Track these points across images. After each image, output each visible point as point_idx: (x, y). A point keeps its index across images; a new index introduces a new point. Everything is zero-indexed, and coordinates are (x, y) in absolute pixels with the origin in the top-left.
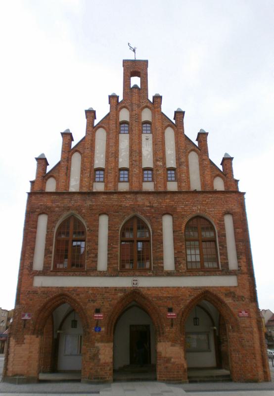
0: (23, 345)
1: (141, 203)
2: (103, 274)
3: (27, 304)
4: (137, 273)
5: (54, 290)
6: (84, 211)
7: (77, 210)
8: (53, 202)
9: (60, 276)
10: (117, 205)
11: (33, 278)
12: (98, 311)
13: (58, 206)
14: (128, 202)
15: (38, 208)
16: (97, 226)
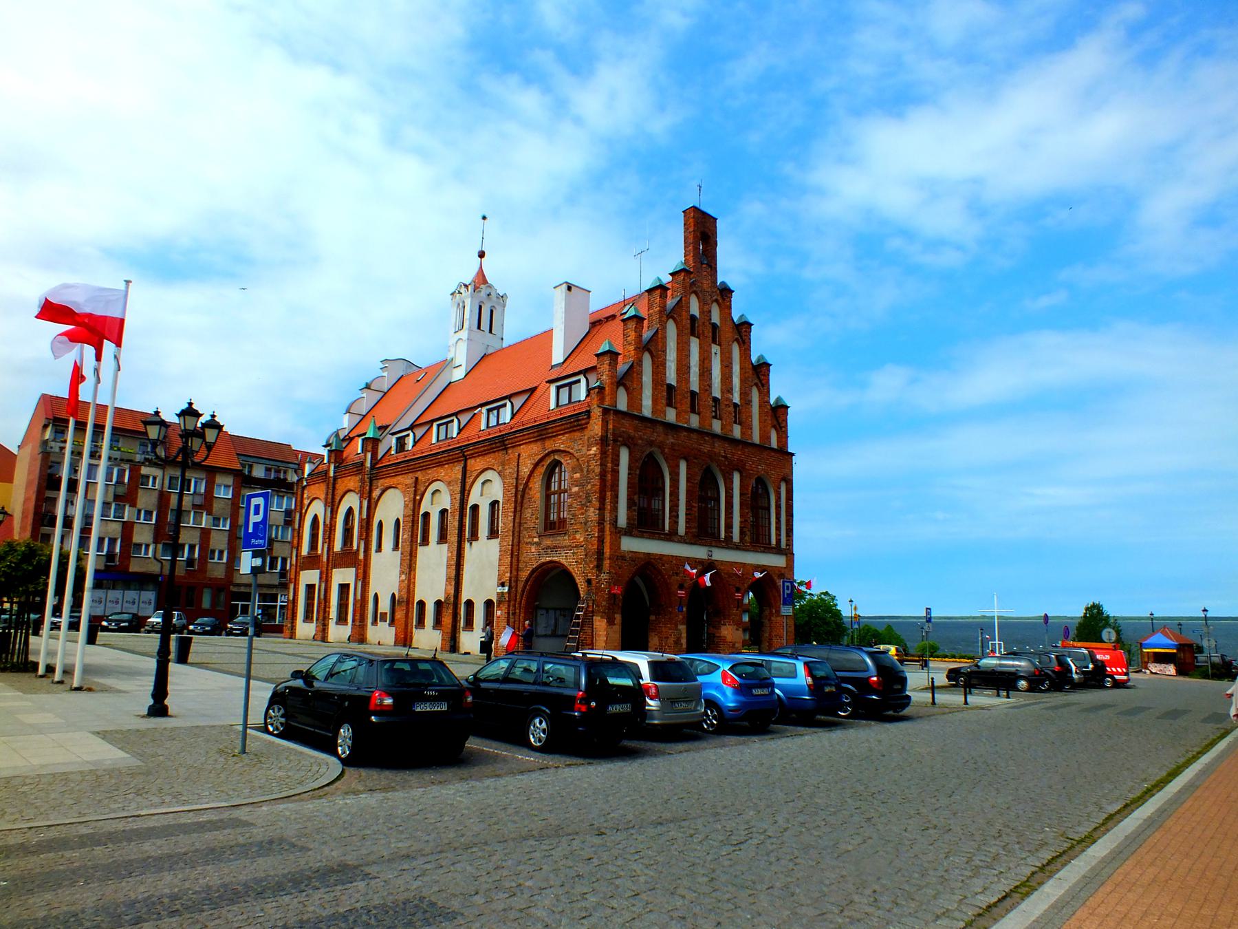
0: (614, 627)
1: (717, 451)
2: (682, 541)
3: (616, 573)
4: (714, 543)
5: (642, 556)
6: (666, 450)
7: (660, 447)
8: (636, 429)
9: (647, 538)
10: (697, 449)
11: (620, 538)
12: (681, 587)
13: (641, 438)
14: (706, 448)
15: (620, 437)
16: (678, 474)
